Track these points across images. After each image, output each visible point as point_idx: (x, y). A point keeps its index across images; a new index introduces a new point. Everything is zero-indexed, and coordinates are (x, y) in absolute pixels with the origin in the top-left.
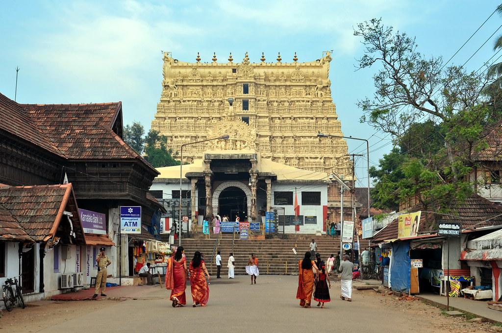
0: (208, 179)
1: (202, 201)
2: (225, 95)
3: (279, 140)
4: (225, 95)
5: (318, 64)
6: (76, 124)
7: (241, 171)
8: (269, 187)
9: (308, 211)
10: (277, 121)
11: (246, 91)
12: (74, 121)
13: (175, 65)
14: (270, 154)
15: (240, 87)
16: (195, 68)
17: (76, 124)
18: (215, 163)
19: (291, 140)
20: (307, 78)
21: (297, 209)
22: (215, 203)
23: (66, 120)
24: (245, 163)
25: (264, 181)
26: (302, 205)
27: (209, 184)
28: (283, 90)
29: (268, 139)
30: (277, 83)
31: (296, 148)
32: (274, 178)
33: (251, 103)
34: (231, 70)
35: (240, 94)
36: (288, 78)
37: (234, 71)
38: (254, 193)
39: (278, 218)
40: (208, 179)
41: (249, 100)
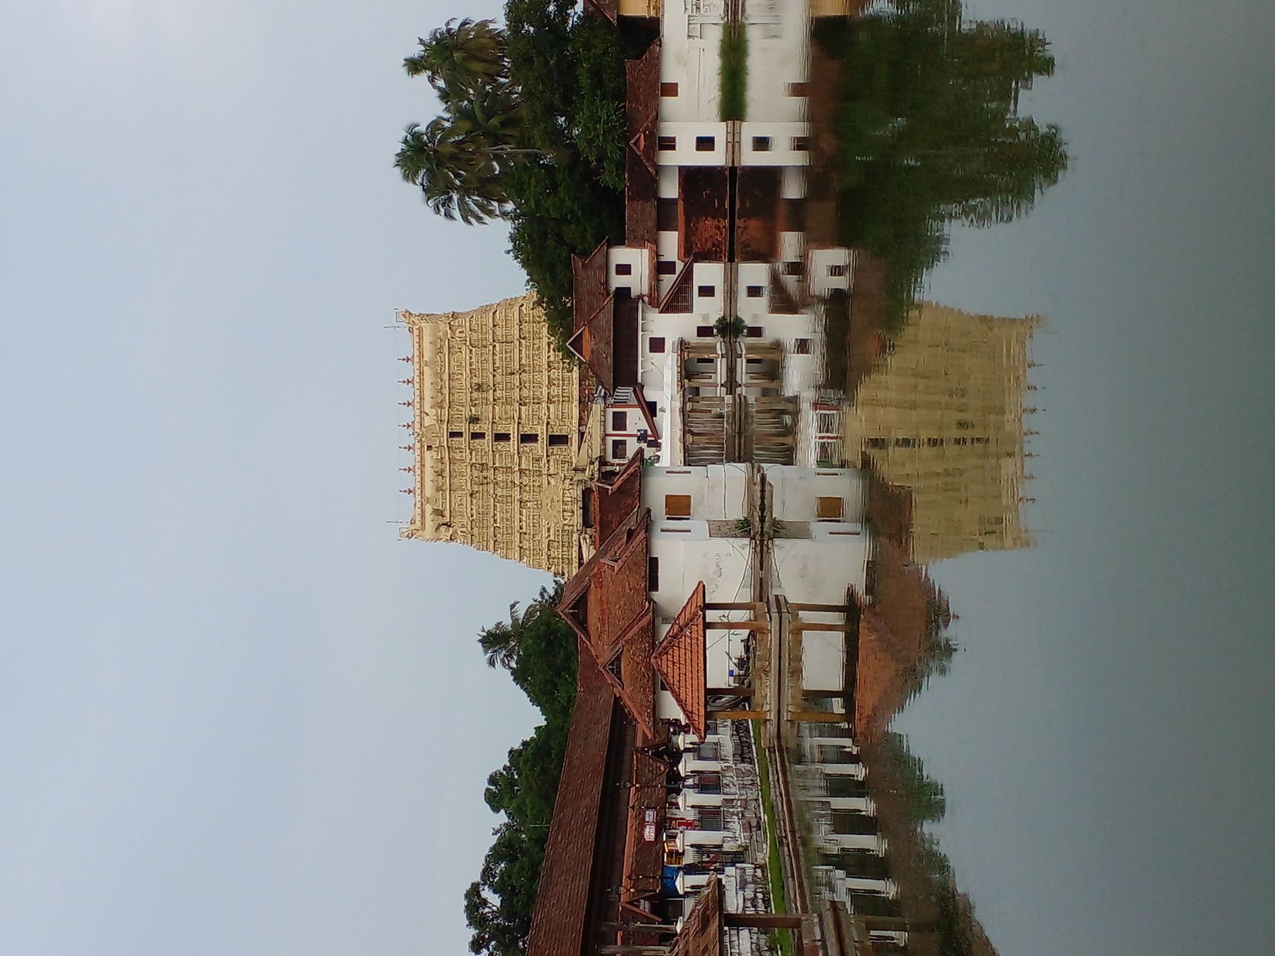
2: (462, 461)
3: (525, 393)
4: (462, 461)
5: (416, 332)
10: (499, 394)
11: (460, 434)
13: (418, 524)
14: (544, 405)
16: (424, 501)
18: (586, 523)
19: (525, 376)
20: (439, 351)
24: (587, 493)
28: (455, 384)
29: (523, 408)
30: (446, 391)
31: (536, 369)
33: (476, 428)
34: (428, 454)
35: (463, 442)
36: (439, 375)
37: (429, 448)
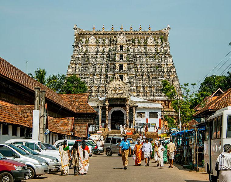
0: (107, 107)
1: (104, 116)
6: (76, 101)
7: (121, 103)
8: (134, 110)
9: (152, 121)
12: (76, 100)
15: (118, 47)
17: (76, 101)
18: (110, 100)
21: (147, 120)
22: (110, 118)
23: (73, 99)
24: (125, 100)
25: (132, 108)
26: (150, 118)
27: (107, 109)
32: (136, 107)
38: (128, 113)
39: (138, 124)
40: (107, 107)
41: (124, 55)
